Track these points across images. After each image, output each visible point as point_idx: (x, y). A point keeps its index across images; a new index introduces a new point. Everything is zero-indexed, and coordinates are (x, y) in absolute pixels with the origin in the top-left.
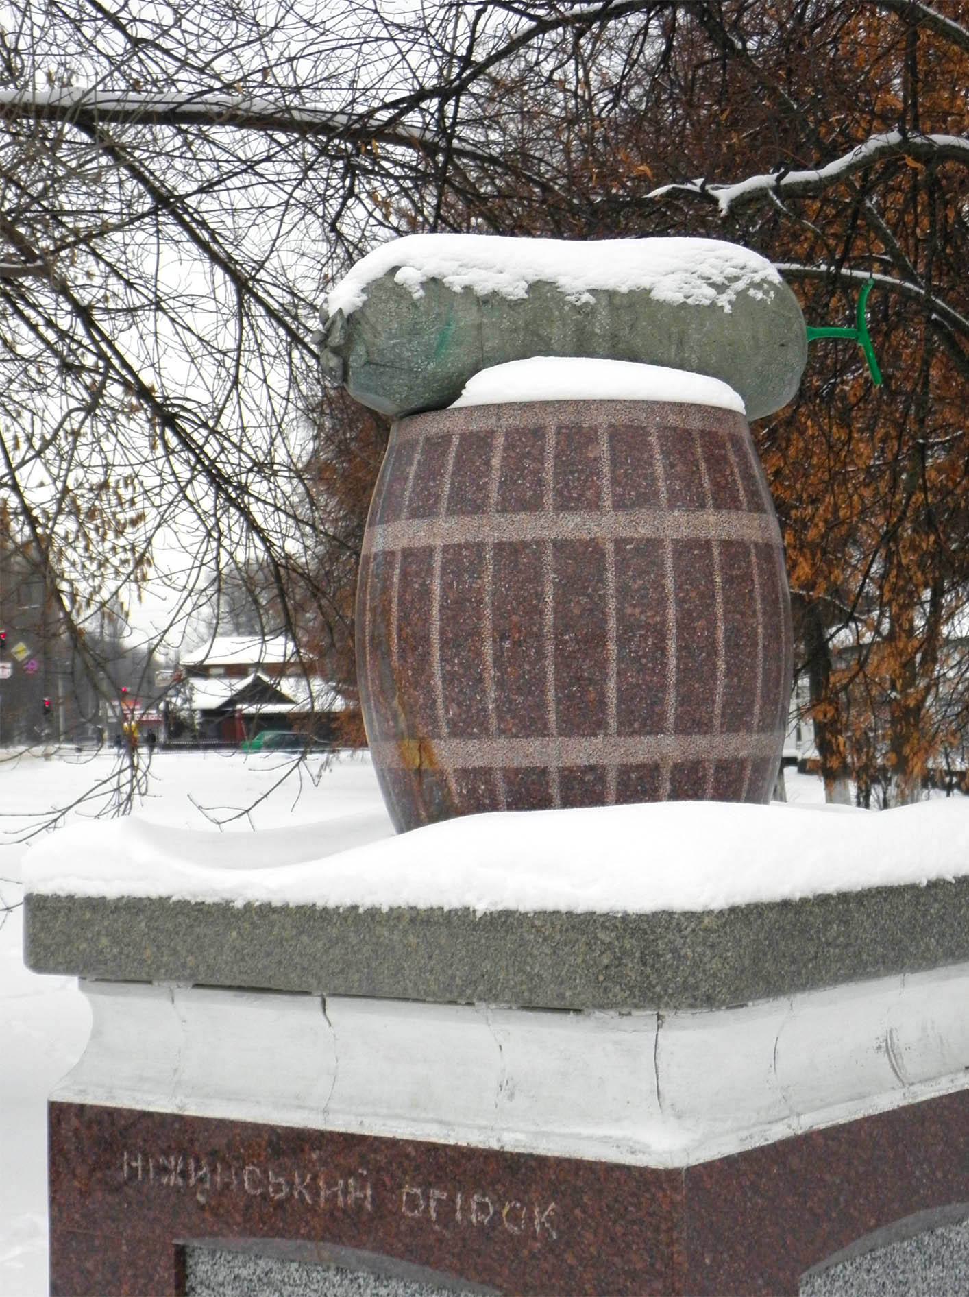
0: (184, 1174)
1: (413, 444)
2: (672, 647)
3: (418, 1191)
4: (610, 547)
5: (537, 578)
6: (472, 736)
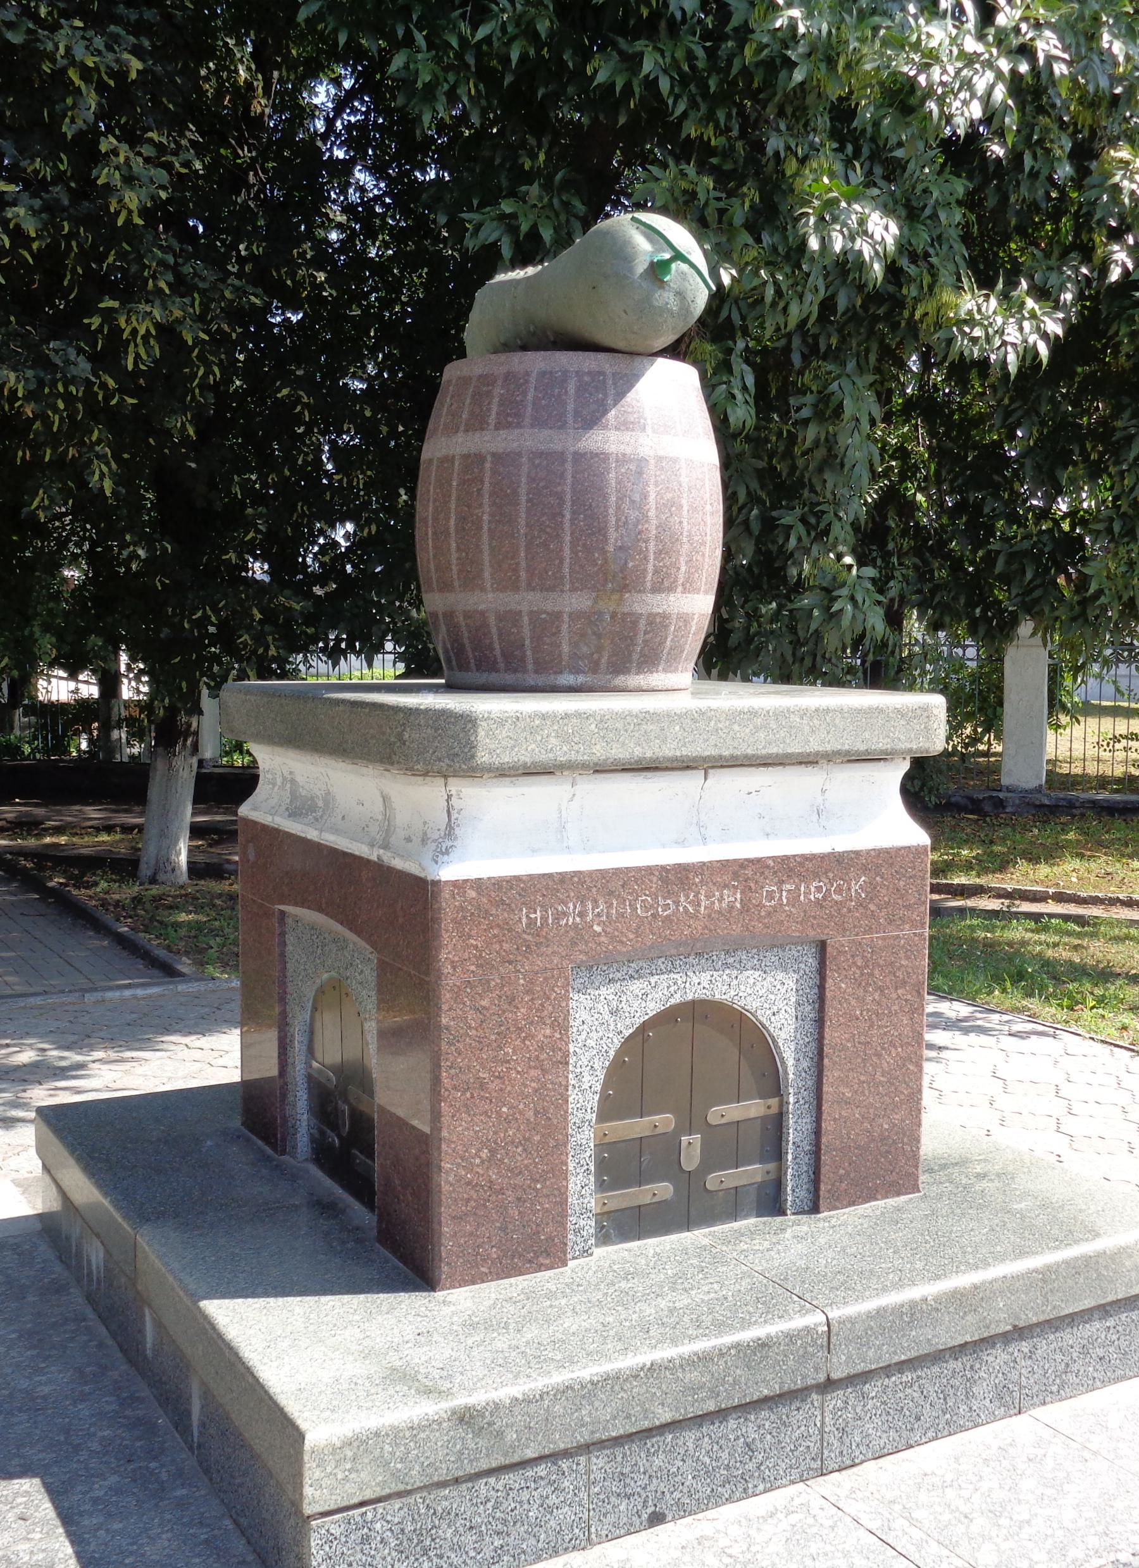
0: (582, 914)
3: (775, 888)
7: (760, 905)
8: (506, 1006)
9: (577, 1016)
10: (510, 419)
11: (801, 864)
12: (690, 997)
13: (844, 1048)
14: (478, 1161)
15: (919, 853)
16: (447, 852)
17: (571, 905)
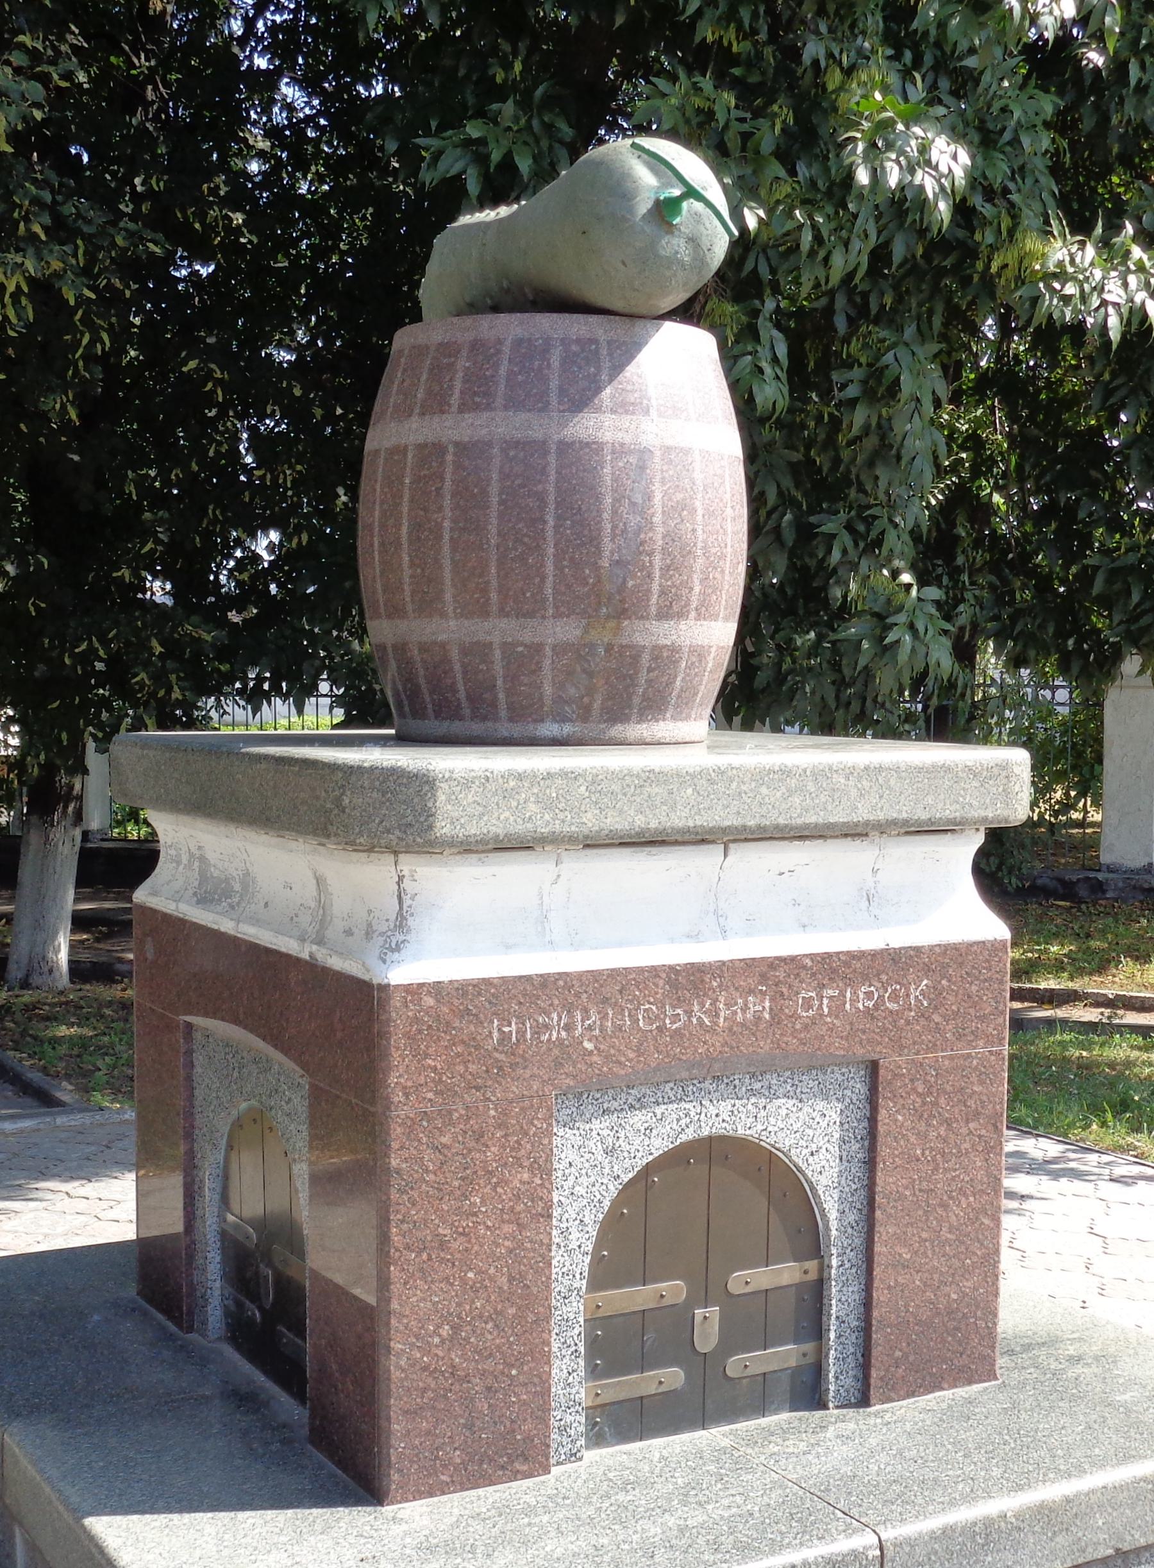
0: (569, 1028)
3: (813, 994)
7: (794, 1016)
8: (473, 1144)
9: (563, 1156)
10: (477, 399)
11: (847, 964)
12: (706, 1132)
13: (901, 1197)
14: (437, 1340)
15: (997, 949)
16: (398, 949)
17: (555, 1016)
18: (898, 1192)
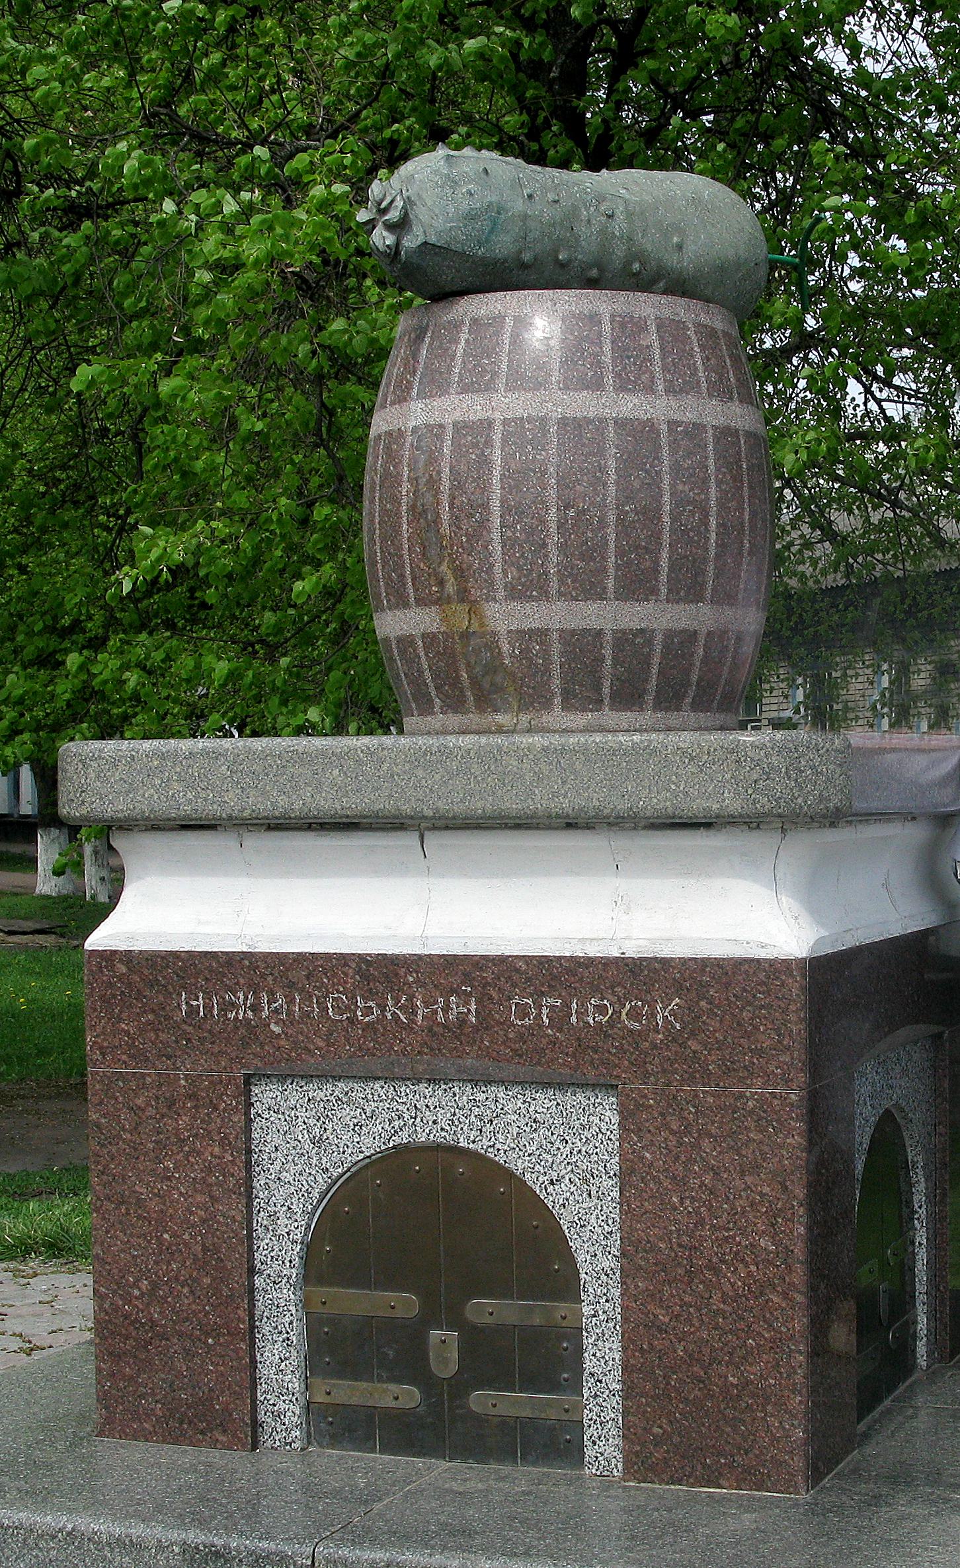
1: (457, 326)
2: (713, 523)
4: (664, 427)
5: (601, 452)
6: (531, 598)
7: (507, 1024)
9: (269, 1138)
11: (569, 971)
14: (136, 1292)
18: (649, 1242)
